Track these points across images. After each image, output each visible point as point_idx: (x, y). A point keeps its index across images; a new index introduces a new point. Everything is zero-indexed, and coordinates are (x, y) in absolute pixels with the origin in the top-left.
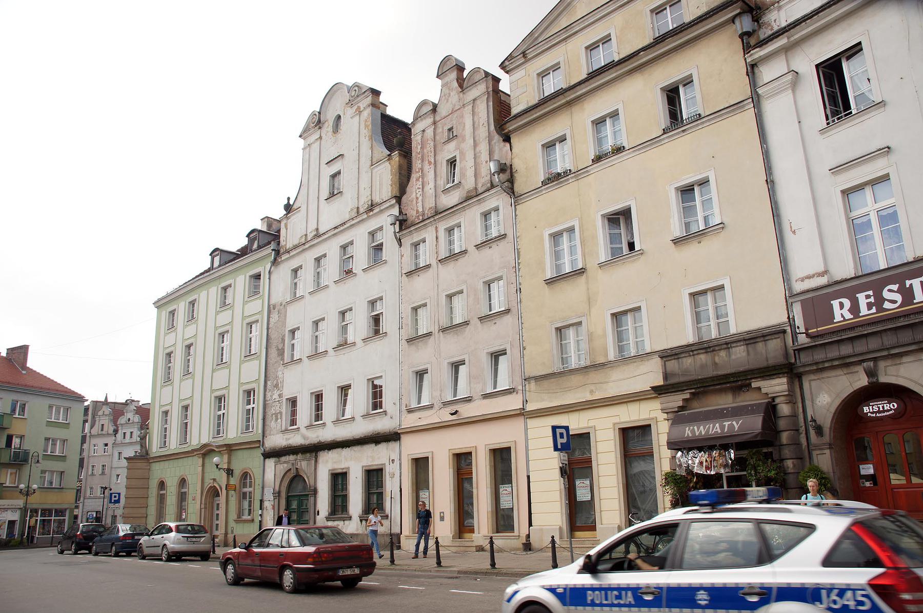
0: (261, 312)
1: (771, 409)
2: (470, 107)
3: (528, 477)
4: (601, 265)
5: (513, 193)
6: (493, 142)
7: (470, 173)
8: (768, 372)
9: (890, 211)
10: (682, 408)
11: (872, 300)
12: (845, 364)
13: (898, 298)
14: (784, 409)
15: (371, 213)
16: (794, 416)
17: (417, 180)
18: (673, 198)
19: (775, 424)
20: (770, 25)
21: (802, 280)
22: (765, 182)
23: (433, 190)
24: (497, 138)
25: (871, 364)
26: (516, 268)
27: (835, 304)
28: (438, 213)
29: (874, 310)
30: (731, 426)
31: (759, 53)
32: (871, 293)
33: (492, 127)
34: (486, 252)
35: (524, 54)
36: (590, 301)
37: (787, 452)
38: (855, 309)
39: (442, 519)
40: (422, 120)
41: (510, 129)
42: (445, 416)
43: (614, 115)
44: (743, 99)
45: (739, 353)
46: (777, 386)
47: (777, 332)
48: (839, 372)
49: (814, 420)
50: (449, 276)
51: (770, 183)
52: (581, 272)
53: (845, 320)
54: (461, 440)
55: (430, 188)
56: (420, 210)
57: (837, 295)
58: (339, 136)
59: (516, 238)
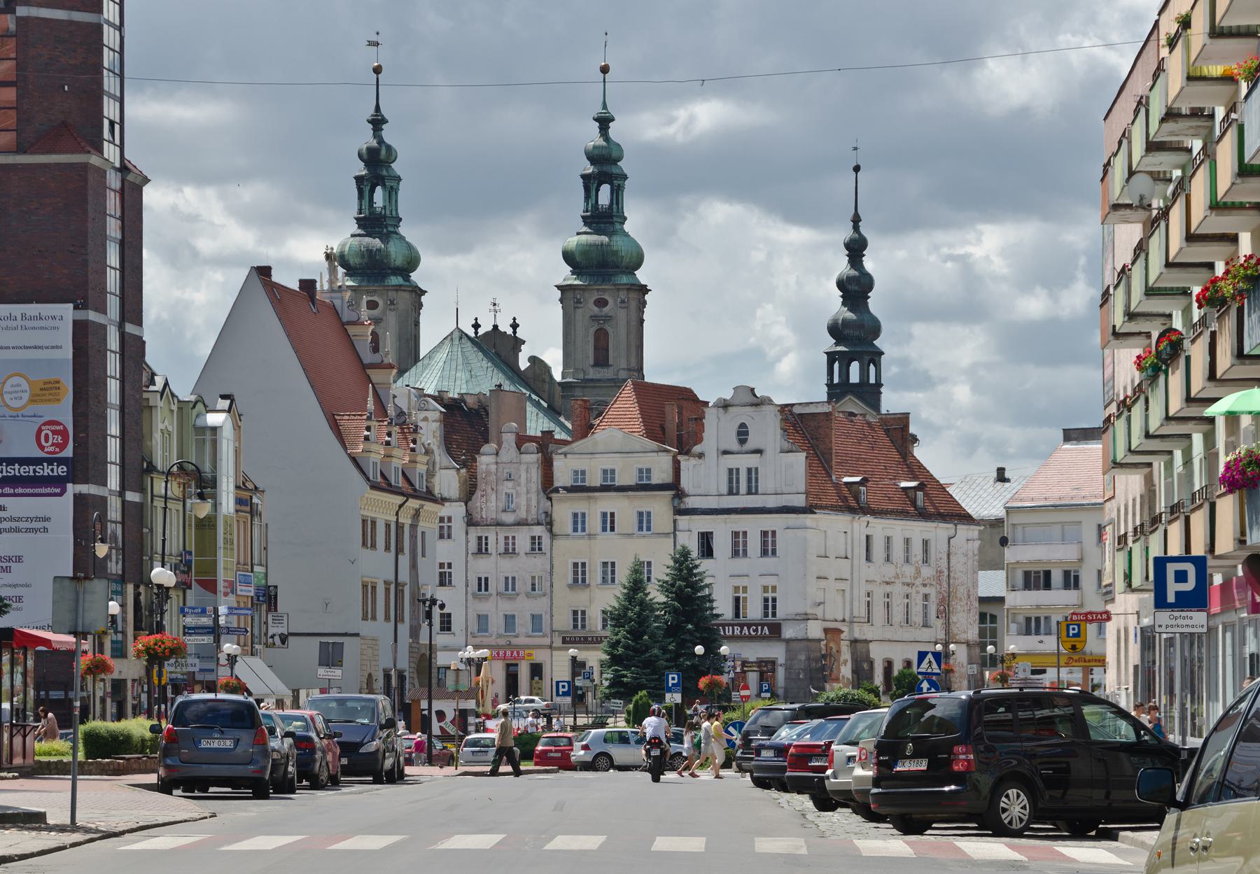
7: (524, 508)
17: (482, 496)
23: (494, 508)
24: (542, 494)
26: (551, 573)
28: (499, 524)
55: (492, 504)
56: (484, 517)
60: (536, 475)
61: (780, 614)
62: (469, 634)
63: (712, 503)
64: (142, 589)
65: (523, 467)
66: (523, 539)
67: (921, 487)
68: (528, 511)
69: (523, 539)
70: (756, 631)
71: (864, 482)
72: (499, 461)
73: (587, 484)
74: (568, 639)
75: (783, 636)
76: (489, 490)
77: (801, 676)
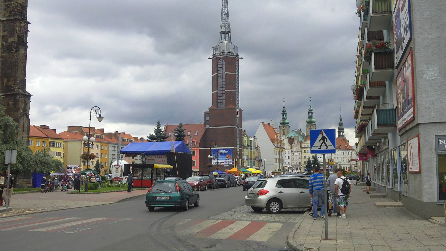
28: (295, 152)
60: (299, 146)
64: (242, 160)
66: (298, 153)
67: (348, 146)
71: (340, 146)
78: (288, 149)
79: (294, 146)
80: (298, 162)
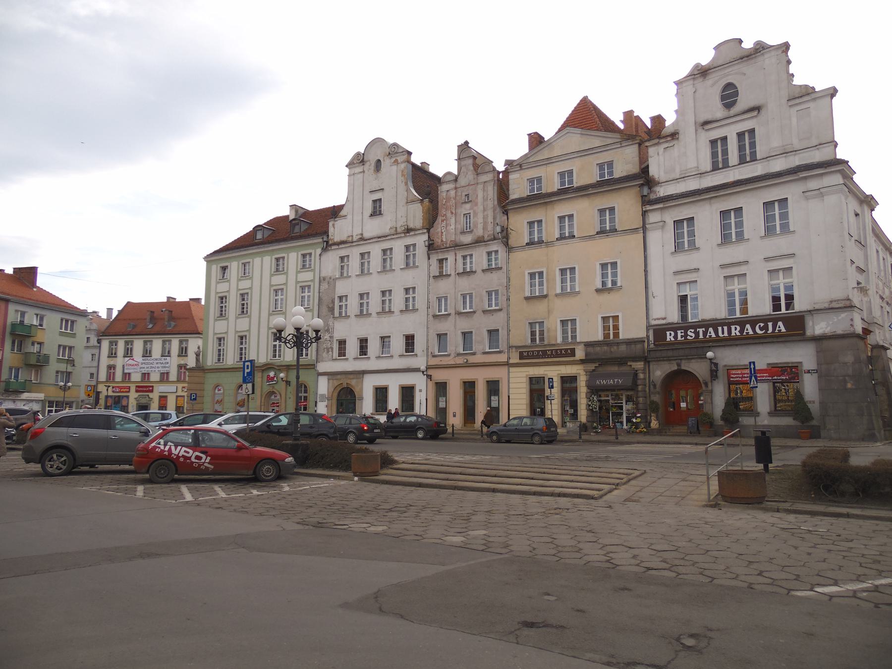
0: (313, 281)
1: (636, 375)
2: (482, 186)
3: (509, 397)
4: (557, 295)
5: (508, 245)
6: (496, 212)
7: (480, 226)
8: (635, 359)
9: (695, 296)
10: (594, 370)
11: (683, 334)
12: (669, 359)
13: (693, 335)
14: (641, 376)
15: (408, 234)
16: (645, 379)
17: (443, 221)
18: (598, 268)
19: (636, 382)
20: (656, 193)
21: (655, 320)
22: (643, 271)
23: (453, 231)
24: (498, 210)
25: (679, 361)
26: (508, 287)
27: (668, 333)
28: (457, 246)
29: (683, 339)
30: (618, 381)
31: (649, 208)
32: (683, 331)
33: (496, 203)
34: (488, 275)
35: (521, 166)
36: (549, 312)
37: (640, 394)
38: (676, 337)
39: (454, 416)
40: (447, 184)
41: (509, 208)
42: (460, 360)
43: (571, 216)
44: (638, 227)
45: (623, 348)
46: (639, 365)
47: (640, 341)
48: (666, 362)
49: (653, 382)
50: (465, 284)
51: (646, 271)
52: (546, 296)
53: (671, 341)
54: (469, 374)
56: (444, 240)
57: (669, 330)
58: (379, 175)
59: (508, 271)
61: (799, 305)
62: (430, 353)
63: (693, 185)
65: (480, 187)
68: (484, 228)
69: (479, 258)
70: (766, 328)
72: (458, 186)
73: (543, 191)
74: (525, 354)
75: (809, 333)
76: (449, 215)
77: (849, 386)
78: (408, 231)
79: (448, 199)
80: (480, 326)
